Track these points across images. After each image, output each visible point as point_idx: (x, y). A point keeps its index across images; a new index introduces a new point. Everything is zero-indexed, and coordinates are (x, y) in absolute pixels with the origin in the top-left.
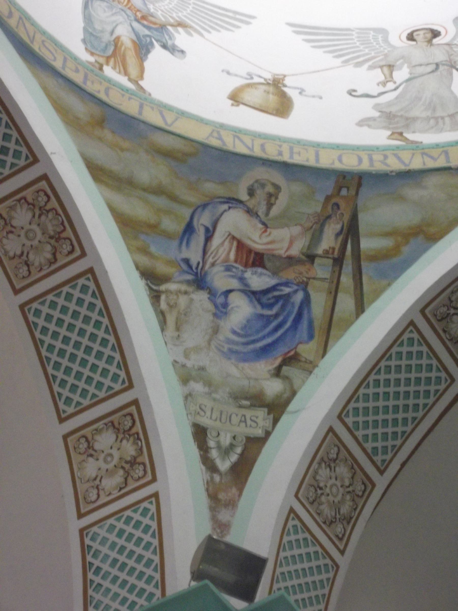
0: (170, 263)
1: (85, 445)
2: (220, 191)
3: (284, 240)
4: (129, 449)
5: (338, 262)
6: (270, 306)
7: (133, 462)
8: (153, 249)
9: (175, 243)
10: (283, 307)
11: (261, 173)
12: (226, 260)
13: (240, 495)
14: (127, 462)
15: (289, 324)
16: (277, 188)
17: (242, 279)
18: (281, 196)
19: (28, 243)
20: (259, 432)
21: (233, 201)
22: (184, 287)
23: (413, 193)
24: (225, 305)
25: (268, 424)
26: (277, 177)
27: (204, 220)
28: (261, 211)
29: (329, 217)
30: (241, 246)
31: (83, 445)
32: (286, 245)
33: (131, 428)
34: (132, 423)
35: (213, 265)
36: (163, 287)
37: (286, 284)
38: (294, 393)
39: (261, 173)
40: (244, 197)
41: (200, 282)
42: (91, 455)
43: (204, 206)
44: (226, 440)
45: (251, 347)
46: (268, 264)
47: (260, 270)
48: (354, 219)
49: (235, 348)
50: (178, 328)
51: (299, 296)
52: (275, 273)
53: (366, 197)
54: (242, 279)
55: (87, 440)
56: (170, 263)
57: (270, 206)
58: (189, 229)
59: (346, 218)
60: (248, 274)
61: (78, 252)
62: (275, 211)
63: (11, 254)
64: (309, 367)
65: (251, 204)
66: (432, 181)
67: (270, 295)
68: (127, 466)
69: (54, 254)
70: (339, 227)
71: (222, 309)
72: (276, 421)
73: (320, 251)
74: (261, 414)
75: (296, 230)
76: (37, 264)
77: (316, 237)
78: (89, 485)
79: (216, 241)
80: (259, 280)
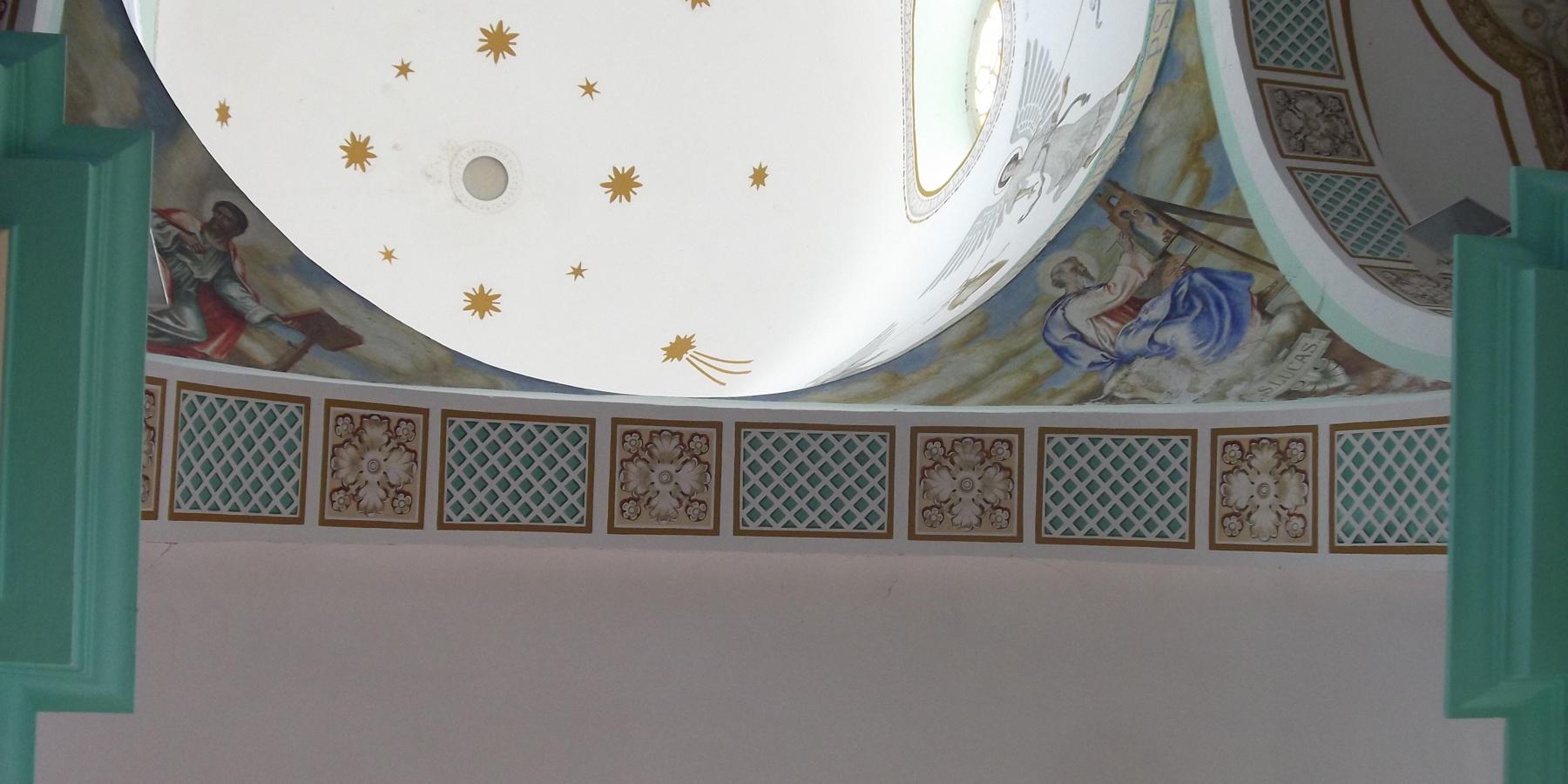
0: (1084, 378)
1: (1234, 519)
2: (1039, 311)
3: (1129, 273)
4: (1265, 457)
5: (1183, 230)
6: (1192, 307)
7: (1282, 455)
8: (1059, 387)
9: (1067, 367)
10: (1200, 296)
11: (1046, 268)
12: (1116, 332)
13: (1384, 366)
14: (1278, 466)
15: (1222, 296)
16: (1069, 260)
17: (1146, 324)
18: (1081, 260)
19: (974, 493)
20: (1324, 344)
21: (1059, 303)
22: (1120, 375)
23: (1155, 138)
24: (1164, 346)
25: (1319, 333)
26: (1061, 255)
27: (1060, 336)
28: (1085, 282)
29: (1132, 224)
30: (1111, 314)
31: (1233, 522)
32: (1135, 273)
33: (1241, 449)
34: (1237, 446)
35: (1113, 344)
36: (1107, 391)
37: (1178, 285)
38: (1301, 304)
39: (1046, 268)
40: (1062, 292)
41: (1123, 361)
42: (1250, 514)
43: (1046, 329)
44: (1315, 376)
45: (1225, 335)
46: (1146, 296)
47: (1147, 305)
48: (1147, 201)
49: (1219, 347)
50: (1161, 391)
51: (1199, 278)
52: (1160, 293)
53: (1132, 184)
54: (1146, 324)
55: (1229, 516)
56: (1084, 378)
57: (1085, 273)
58: (1061, 351)
59: (1142, 208)
60: (1144, 317)
61: (1015, 438)
62: (1093, 272)
63: (975, 521)
64: (1282, 284)
65: (1072, 289)
66: (1152, 117)
67: (1180, 306)
68: (1284, 466)
69: (1002, 468)
70: (1147, 219)
71: (1168, 351)
72: (1322, 325)
73: (1162, 244)
74: (1305, 339)
75: (1126, 259)
76: (1001, 495)
77: (1146, 243)
78: (1282, 529)
79: (1090, 333)
80: (1158, 309)
